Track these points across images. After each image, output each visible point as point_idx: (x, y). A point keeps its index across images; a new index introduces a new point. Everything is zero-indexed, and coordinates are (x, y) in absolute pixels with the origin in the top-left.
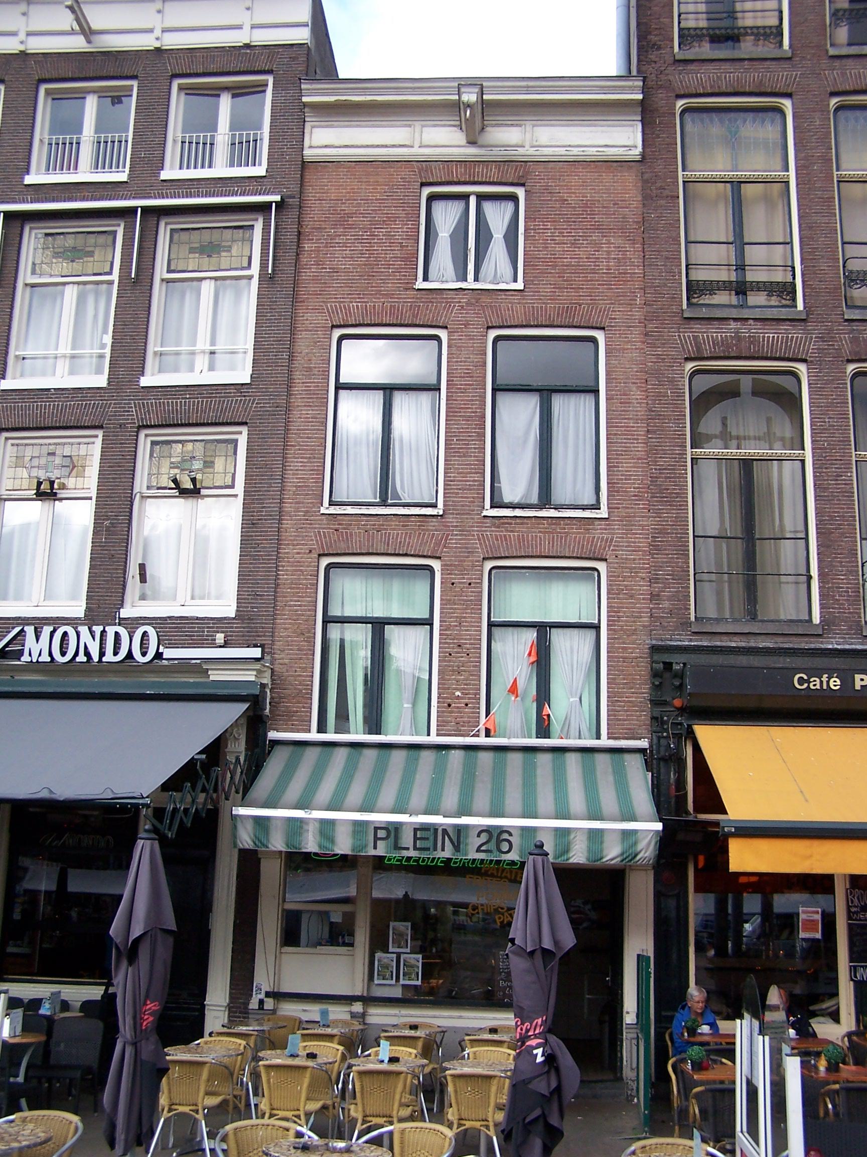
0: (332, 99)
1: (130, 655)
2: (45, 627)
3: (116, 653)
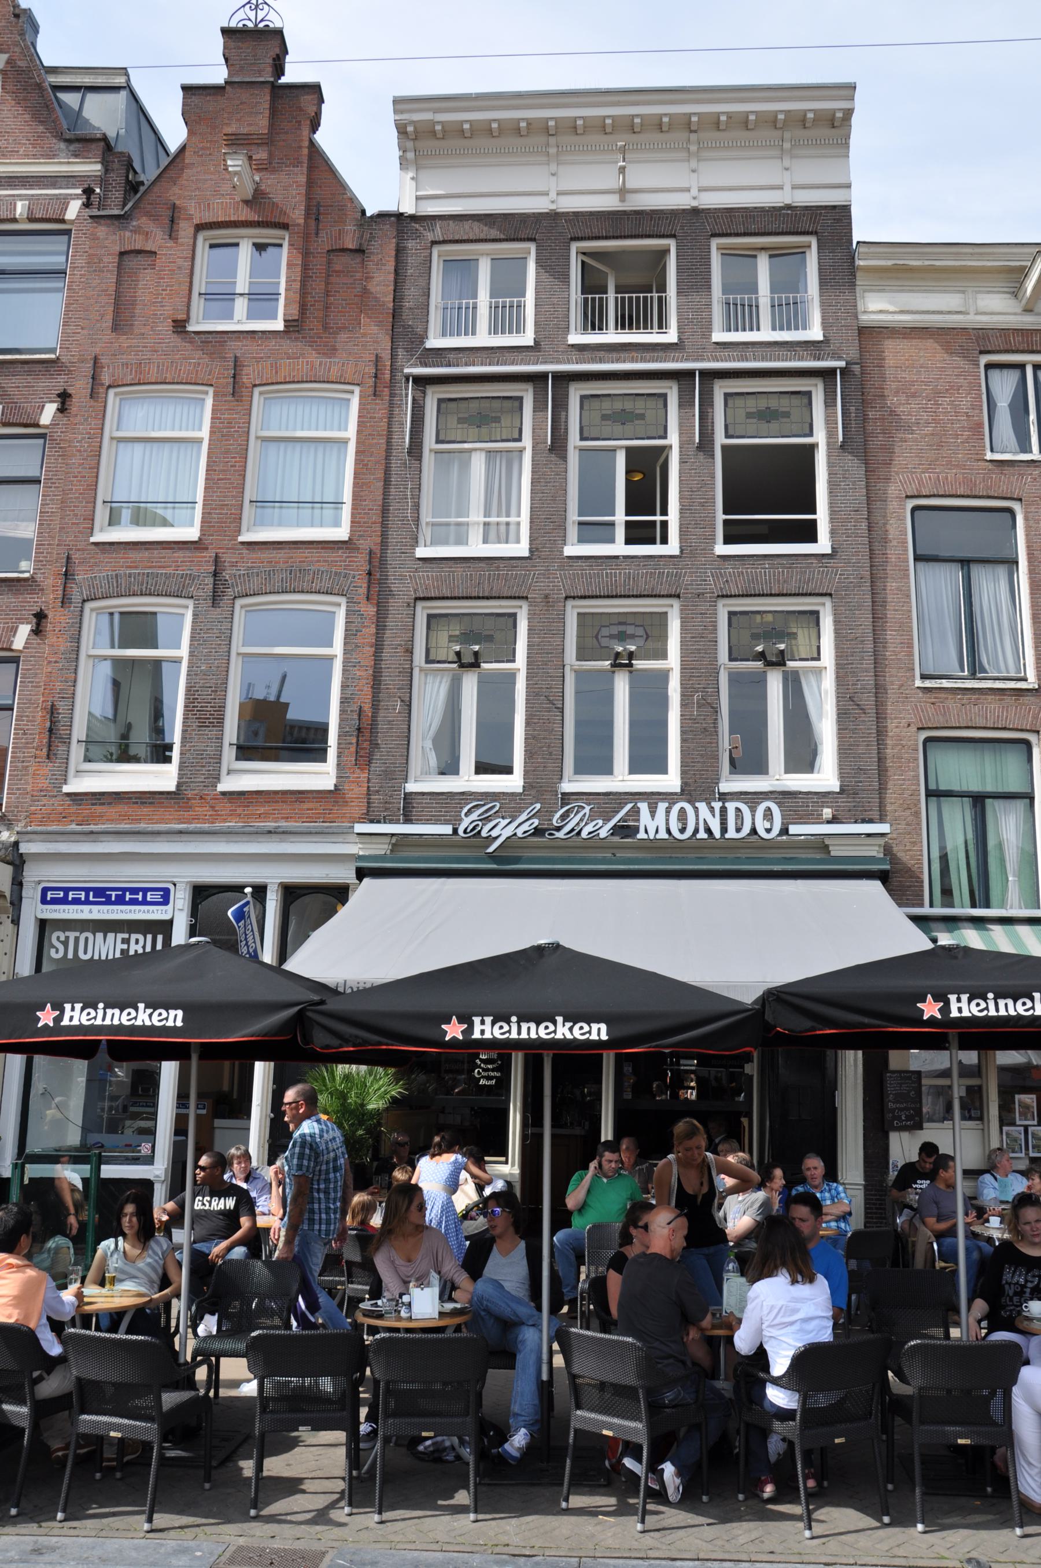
0: (890, 263)
1: (754, 831)
2: (660, 804)
3: (738, 830)
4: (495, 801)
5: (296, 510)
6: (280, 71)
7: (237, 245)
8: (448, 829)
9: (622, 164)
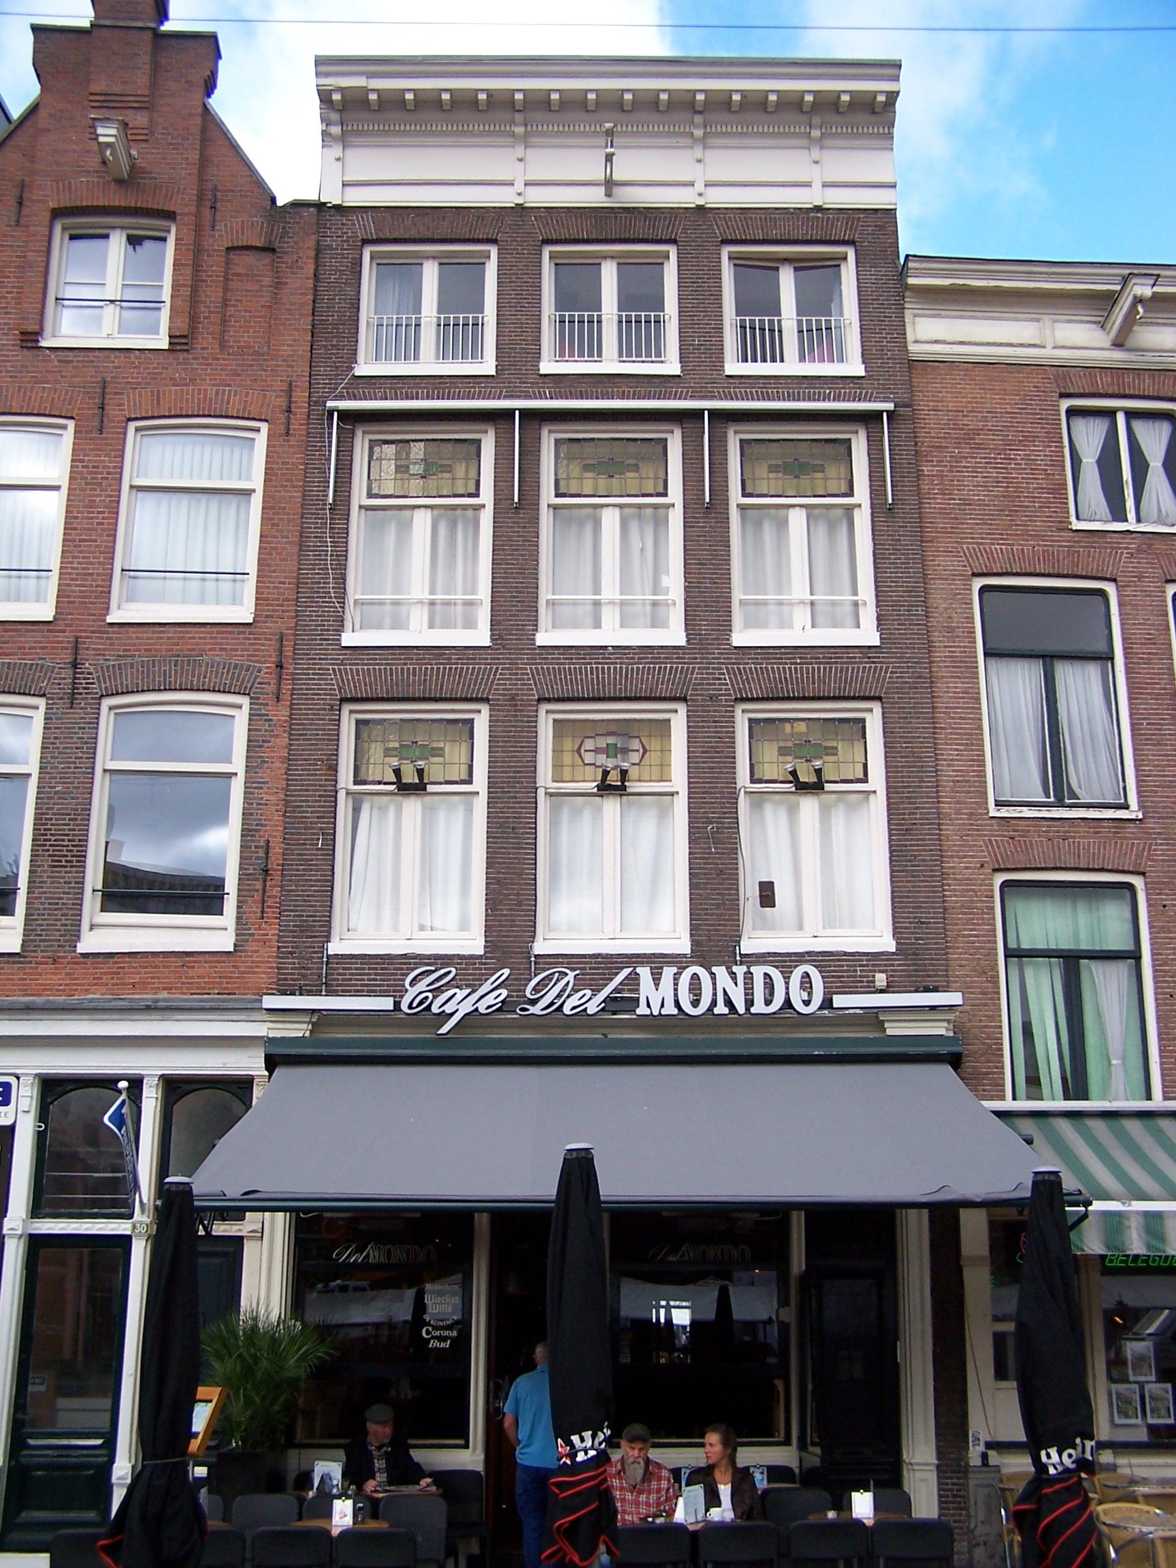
0: (946, 282)
1: (788, 1003)
3: (768, 1002)
4: (448, 965)
5: (180, 583)
6: (163, 15)
7: (107, 237)
8: (387, 1003)
9: (609, 150)
